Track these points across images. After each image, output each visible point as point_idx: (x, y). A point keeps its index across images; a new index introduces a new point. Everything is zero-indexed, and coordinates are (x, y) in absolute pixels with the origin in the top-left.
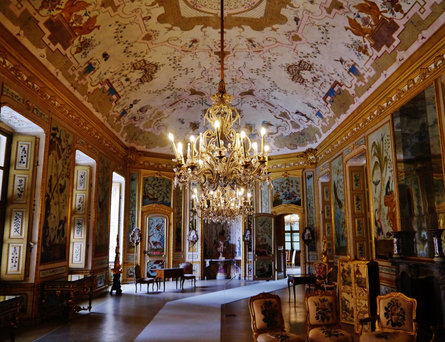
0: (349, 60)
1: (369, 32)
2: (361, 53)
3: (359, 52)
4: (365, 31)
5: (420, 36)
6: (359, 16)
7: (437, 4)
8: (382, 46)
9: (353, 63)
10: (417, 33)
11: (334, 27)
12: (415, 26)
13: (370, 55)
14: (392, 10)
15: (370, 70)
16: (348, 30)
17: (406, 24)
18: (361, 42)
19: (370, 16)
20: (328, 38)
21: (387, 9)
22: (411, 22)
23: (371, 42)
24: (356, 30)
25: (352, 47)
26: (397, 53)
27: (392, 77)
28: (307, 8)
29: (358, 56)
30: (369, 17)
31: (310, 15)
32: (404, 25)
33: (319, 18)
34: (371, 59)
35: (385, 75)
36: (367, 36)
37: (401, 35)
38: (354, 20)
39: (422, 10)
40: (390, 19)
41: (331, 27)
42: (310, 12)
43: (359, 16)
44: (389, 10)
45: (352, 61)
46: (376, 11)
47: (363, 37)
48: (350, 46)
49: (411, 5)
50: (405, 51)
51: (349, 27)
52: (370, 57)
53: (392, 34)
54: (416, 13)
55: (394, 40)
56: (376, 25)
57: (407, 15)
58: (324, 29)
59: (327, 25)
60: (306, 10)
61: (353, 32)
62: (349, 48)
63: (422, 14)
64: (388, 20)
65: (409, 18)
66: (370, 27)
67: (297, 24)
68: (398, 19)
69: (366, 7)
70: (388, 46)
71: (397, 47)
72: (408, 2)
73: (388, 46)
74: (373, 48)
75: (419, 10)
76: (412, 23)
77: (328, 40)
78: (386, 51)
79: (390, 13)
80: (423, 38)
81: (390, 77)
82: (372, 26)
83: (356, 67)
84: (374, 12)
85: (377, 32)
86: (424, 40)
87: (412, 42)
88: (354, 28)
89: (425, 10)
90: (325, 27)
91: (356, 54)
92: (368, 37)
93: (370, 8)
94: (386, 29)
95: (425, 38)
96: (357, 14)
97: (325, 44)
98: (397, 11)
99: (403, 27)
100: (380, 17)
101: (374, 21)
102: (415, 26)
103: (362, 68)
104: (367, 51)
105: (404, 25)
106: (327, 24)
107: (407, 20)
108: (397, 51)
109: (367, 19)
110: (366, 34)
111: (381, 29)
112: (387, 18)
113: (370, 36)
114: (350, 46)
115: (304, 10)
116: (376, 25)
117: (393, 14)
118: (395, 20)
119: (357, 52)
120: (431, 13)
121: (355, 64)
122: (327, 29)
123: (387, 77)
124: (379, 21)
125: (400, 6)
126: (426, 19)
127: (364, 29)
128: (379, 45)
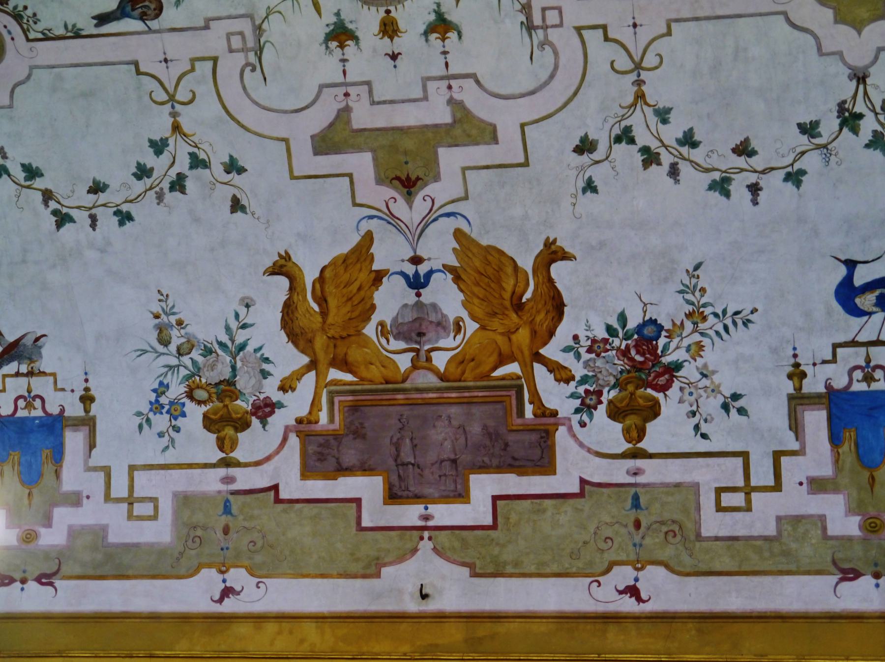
0: (73, 380)
1: (375, 372)
2: (195, 413)
3: (190, 395)
4: (355, 354)
5: (623, 575)
6: (417, 283)
7: (824, 529)
8: (365, 469)
9: (75, 410)
10: (623, 557)
11: (236, 206)
12: (637, 525)
13: (238, 454)
14: (599, 393)
15: (140, 509)
16: (283, 282)
17: (600, 485)
18: (265, 374)
19: (471, 327)
20: (125, 218)
21: (579, 371)
22: (636, 498)
23: (323, 417)
24: (324, 313)
25: (180, 353)
26: (415, 550)
27: (271, 627)
28: (274, 28)
29: (156, 407)
30: (458, 327)
31: (230, 65)
32: (583, 482)
33: (248, 114)
34: (222, 472)
35: (227, 592)
36: (335, 374)
37: (527, 503)
38: (378, 277)
39: (737, 499)
40: (547, 414)
41: (229, 192)
42: (259, 51)
43: (417, 283)
44: (584, 380)
45: (87, 399)
46: (523, 336)
47: (313, 365)
48: (175, 342)
49: (703, 446)
50: (474, 575)
51: (310, 275)
52: (226, 463)
53: (483, 468)
54: (696, 487)
55: (462, 495)
56: (442, 377)
57: (640, 463)
58: (183, 164)
59: (218, 170)
60: (259, 30)
61: (289, 310)
62: (165, 342)
63: (719, 508)
64: (529, 410)
65: (640, 479)
66: (404, 362)
67: (102, 19)
68: (581, 445)
69: (509, 284)
70: (393, 496)
71: (443, 536)
72: (704, 428)
73: (393, 496)
74: (294, 441)
75: (719, 491)
76: (636, 503)
77: (108, 221)
78: (358, 501)
79: (573, 396)
80: (633, 591)
81: (260, 619)
82: (421, 361)
83: (74, 441)
84: (509, 334)
85: (413, 404)
86: (628, 605)
87: (555, 568)
88: (322, 300)
89: (748, 509)
90: (197, 162)
91: (162, 389)
92: (335, 382)
93: (518, 307)
94: (476, 429)
95: (639, 600)
96: (423, 269)
97: (62, 219)
98: (615, 413)
99: (576, 489)
100: (513, 368)
101: (460, 361)
102: (637, 525)
103: (107, 471)
104: (243, 425)
105: (583, 482)
106: (233, 167)
107: (622, 478)
108: (426, 546)
109: (441, 325)
110: (344, 365)
111: (454, 410)
112: (536, 399)
113: (353, 393)
114: (175, 342)
115: (251, 17)
116: (442, 377)
117: (587, 407)
118: (561, 434)
119: (177, 390)
120: (766, 539)
121: (88, 423)
122: (189, 184)
123: (230, 606)
124: (487, 376)
125: (653, 411)
126: (717, 539)
127: (366, 342)
128: (350, 457)
